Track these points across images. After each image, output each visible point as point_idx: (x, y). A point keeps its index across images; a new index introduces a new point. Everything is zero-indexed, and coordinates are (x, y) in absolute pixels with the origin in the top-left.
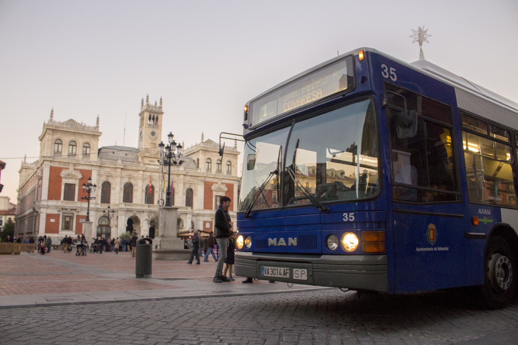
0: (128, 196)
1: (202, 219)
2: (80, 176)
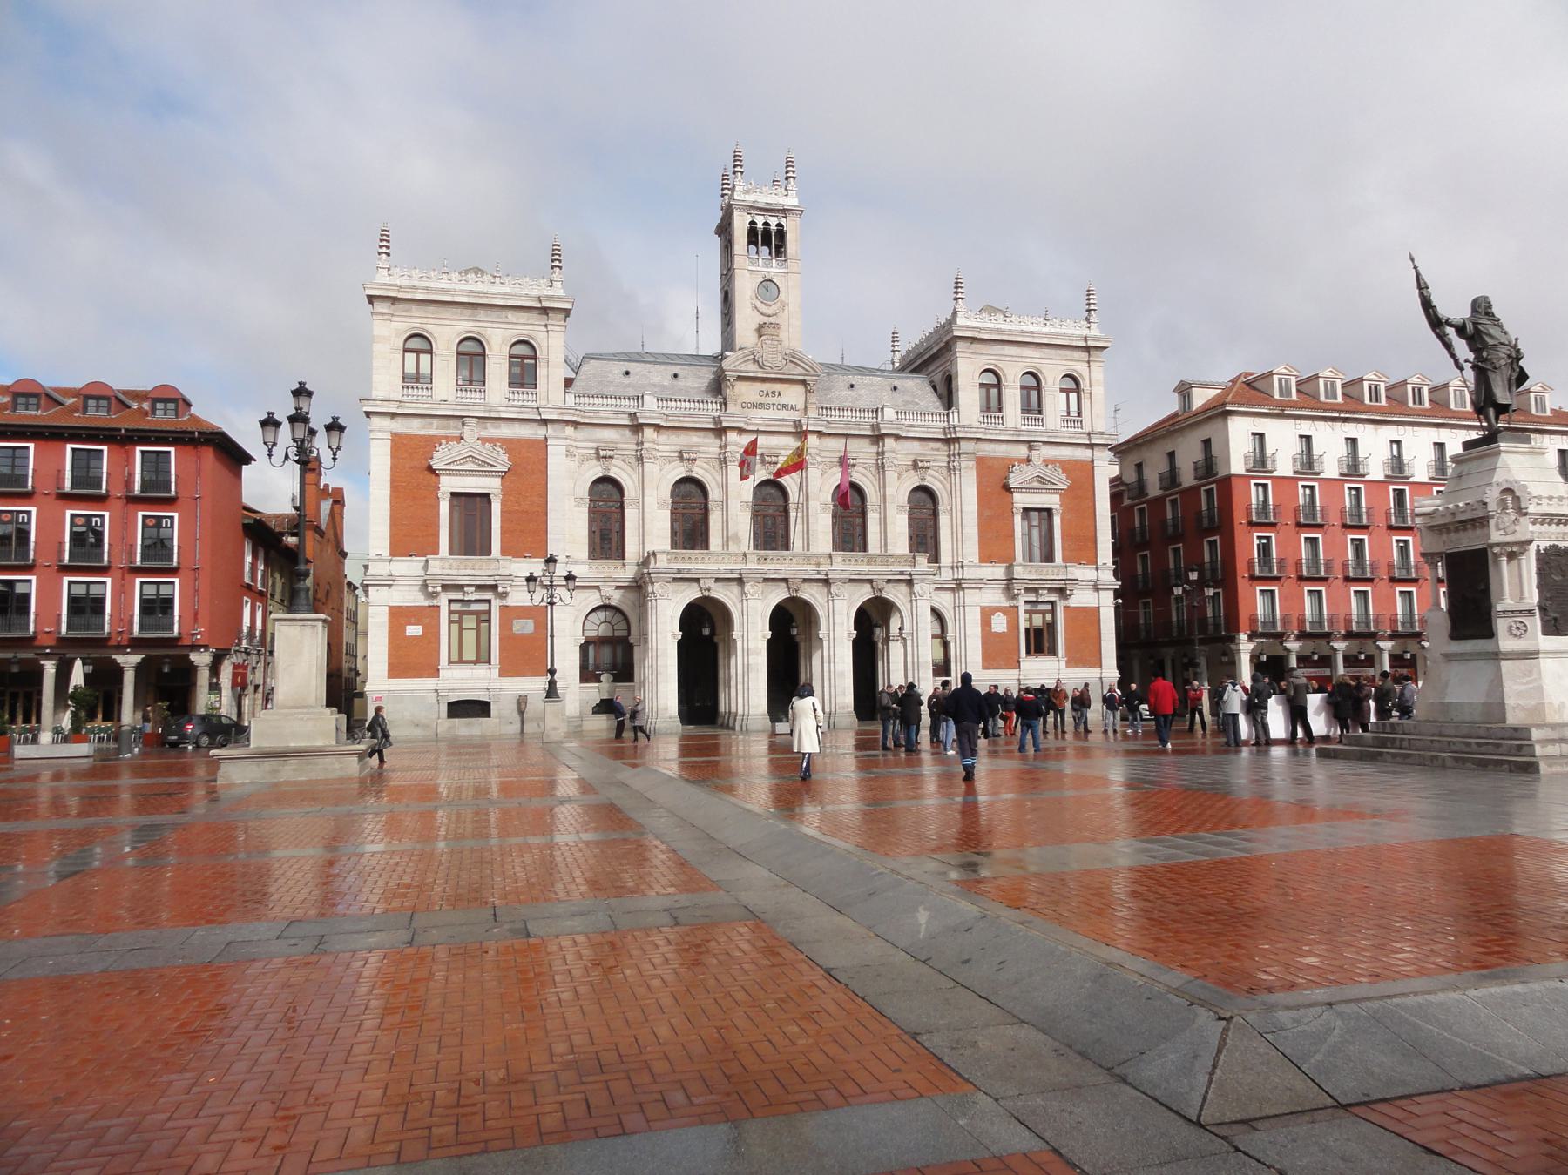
0: (691, 528)
1: (975, 600)
2: (502, 461)
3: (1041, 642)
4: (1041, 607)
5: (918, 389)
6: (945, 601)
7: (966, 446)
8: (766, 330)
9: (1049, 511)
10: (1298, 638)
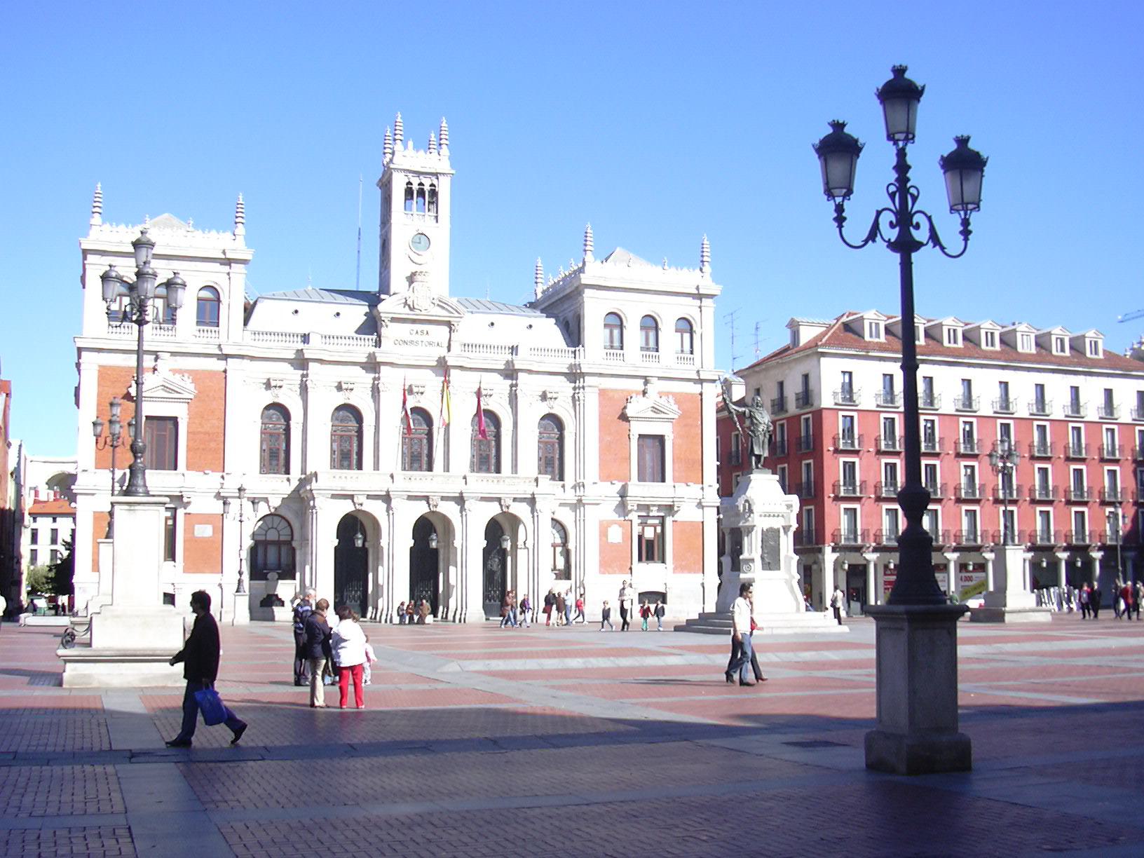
3: (651, 551)
4: (650, 521)
5: (548, 330)
6: (566, 517)
7: (589, 380)
8: (418, 277)
9: (661, 439)
10: (875, 550)
